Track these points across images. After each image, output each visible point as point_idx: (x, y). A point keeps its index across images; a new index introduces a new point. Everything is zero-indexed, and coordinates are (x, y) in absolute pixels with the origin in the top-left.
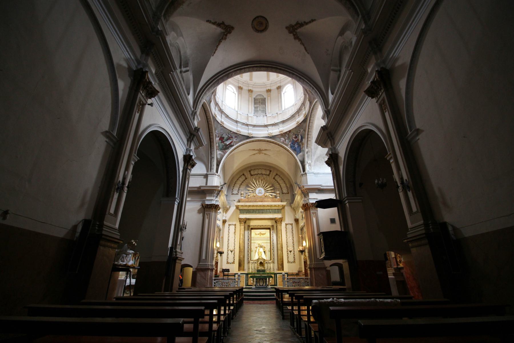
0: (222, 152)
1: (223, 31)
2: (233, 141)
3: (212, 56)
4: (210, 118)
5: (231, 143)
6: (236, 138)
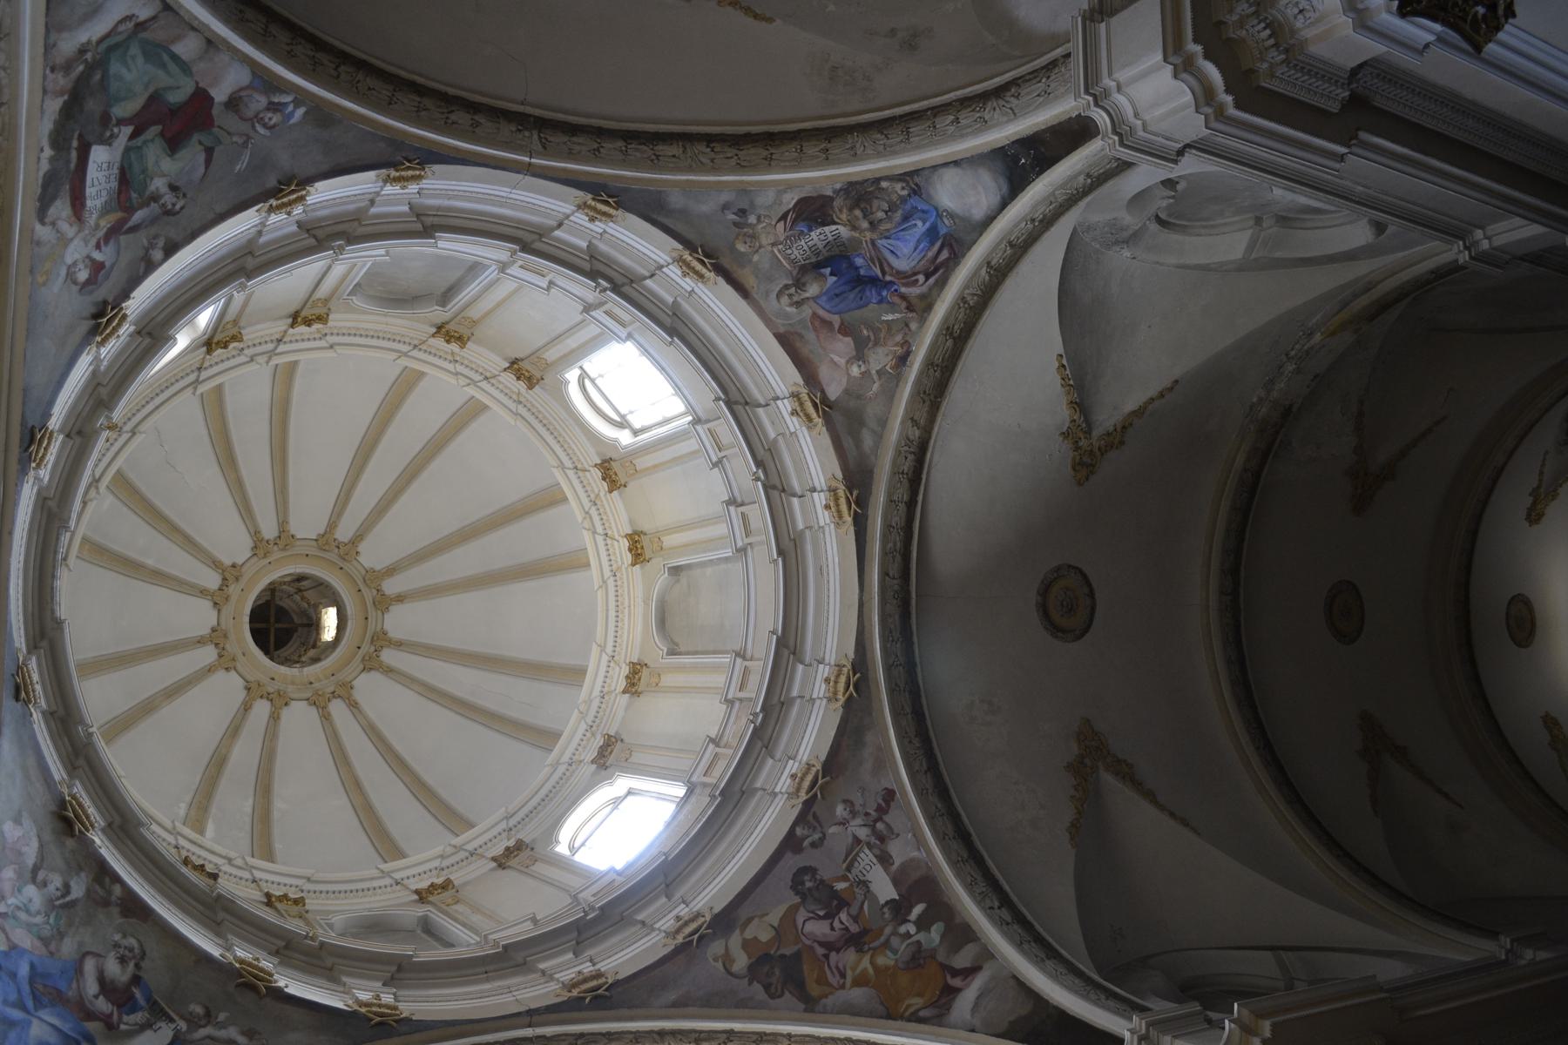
0: (82, 51)
1: (1096, 433)
2: (69, 230)
3: (1062, 351)
4: (448, 128)
5: (78, 201)
6: (83, 275)
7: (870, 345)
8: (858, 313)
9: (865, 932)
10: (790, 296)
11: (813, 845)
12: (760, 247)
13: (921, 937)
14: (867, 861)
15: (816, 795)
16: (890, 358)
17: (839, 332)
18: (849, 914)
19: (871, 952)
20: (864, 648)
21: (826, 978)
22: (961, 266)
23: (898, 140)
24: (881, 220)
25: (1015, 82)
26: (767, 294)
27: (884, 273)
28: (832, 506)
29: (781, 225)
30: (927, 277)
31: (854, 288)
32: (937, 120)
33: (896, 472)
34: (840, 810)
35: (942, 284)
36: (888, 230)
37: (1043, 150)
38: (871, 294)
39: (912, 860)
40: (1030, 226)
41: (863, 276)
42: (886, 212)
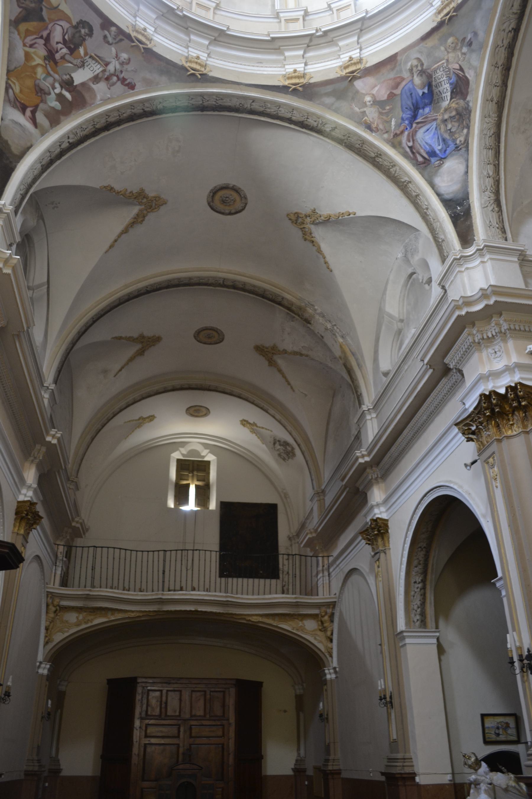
1: (312, 227)
3: (357, 215)
7: (380, 110)
8: (399, 105)
9: (56, 63)
10: (417, 66)
11: (105, 37)
12: (448, 52)
13: (53, 96)
14: (95, 69)
15: (133, 42)
16: (371, 120)
17: (391, 93)
18: (66, 54)
19: (44, 65)
20: (214, 82)
21: (29, 36)
22: (412, 167)
23: (487, 143)
24: (446, 126)
25: (500, 210)
26: (421, 52)
27: (418, 123)
28: (295, 74)
29: (457, 67)
30: (411, 148)
31: (413, 105)
32: (492, 166)
33: (309, 114)
34: (124, 56)
35: (405, 155)
36: (440, 129)
37: (462, 219)
38: (408, 114)
39: (95, 96)
40: (425, 207)
41: (418, 111)
42: (450, 130)
